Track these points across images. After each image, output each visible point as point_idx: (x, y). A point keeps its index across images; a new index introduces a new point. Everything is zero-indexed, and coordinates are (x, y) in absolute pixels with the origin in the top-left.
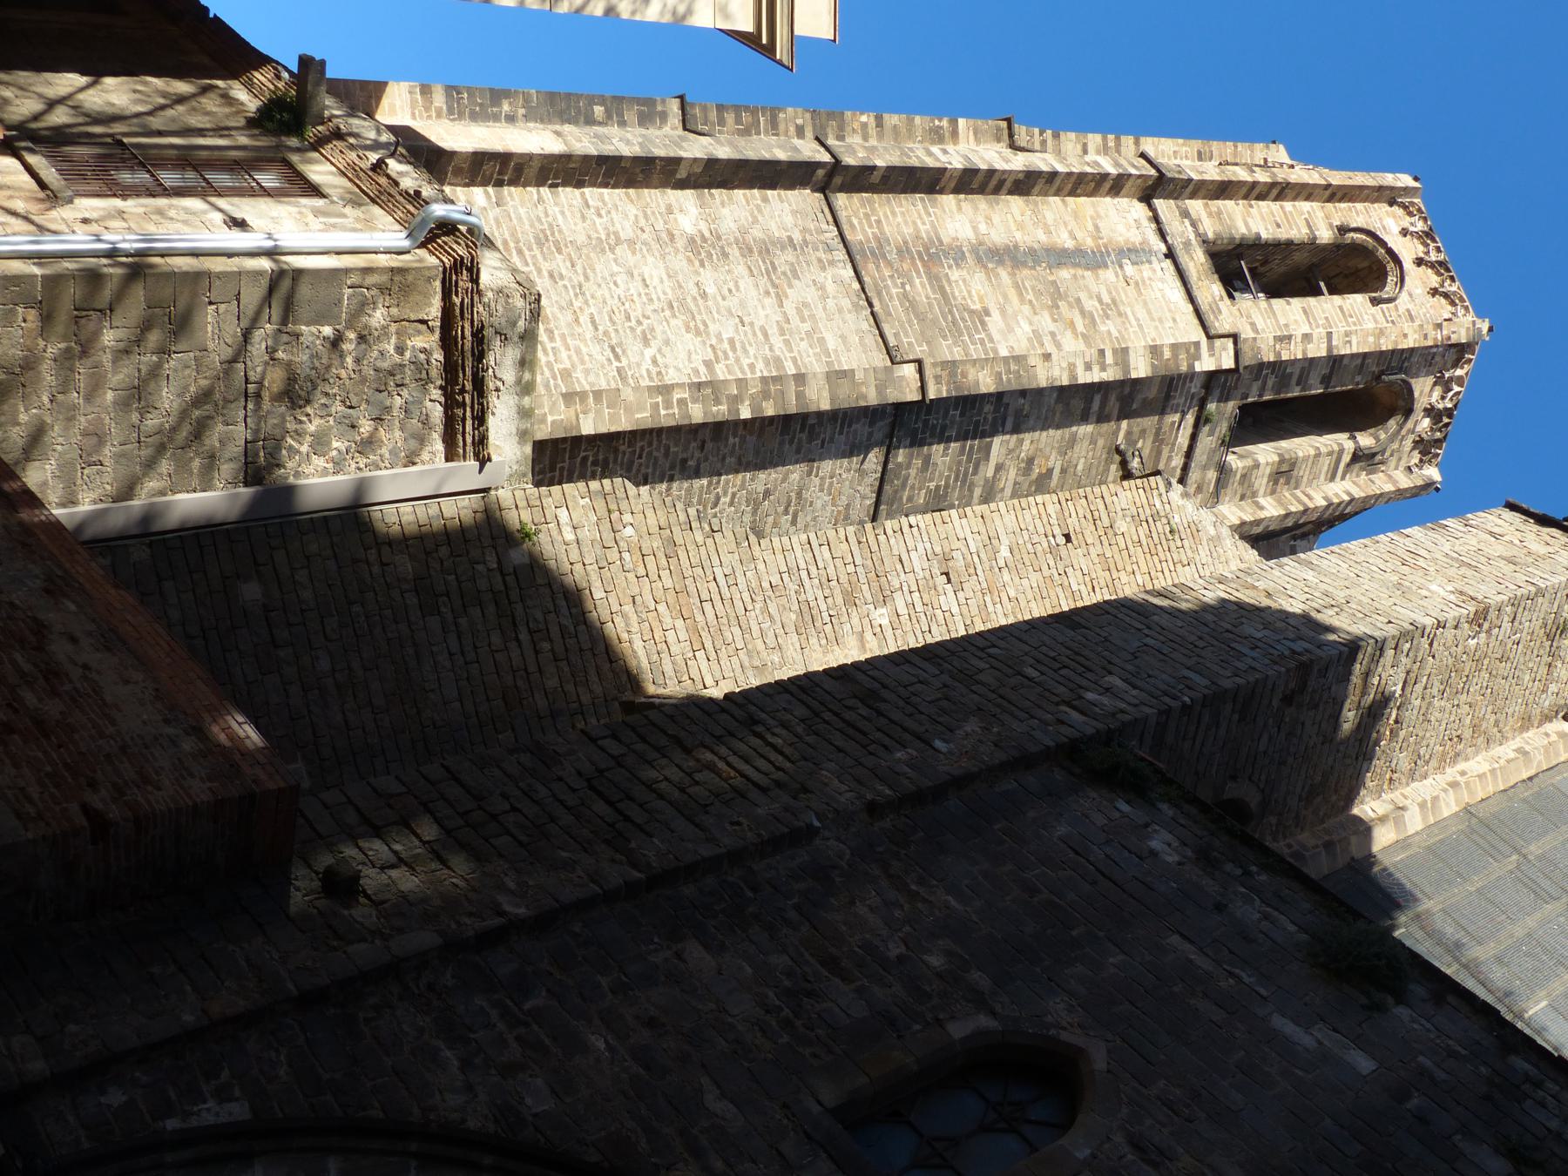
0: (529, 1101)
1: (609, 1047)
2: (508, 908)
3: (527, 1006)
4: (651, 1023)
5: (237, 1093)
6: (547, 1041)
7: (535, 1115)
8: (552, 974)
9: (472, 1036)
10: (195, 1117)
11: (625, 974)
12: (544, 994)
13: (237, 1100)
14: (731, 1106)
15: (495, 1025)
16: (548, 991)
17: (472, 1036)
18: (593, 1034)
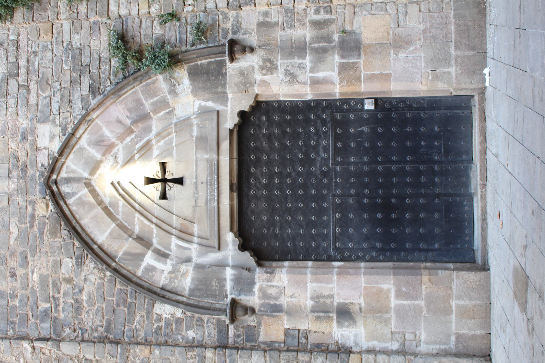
0: (71, 265)
1: (33, 272)
2: (30, 349)
3: (49, 305)
4: (13, 275)
5: (155, 316)
6: (51, 286)
7: (72, 258)
8: (32, 315)
9: (73, 302)
10: (171, 313)
11: (8, 302)
12: (40, 308)
13: (156, 314)
14: (11, 228)
15: (63, 302)
16: (38, 308)
17: (73, 302)
18: (34, 282)
